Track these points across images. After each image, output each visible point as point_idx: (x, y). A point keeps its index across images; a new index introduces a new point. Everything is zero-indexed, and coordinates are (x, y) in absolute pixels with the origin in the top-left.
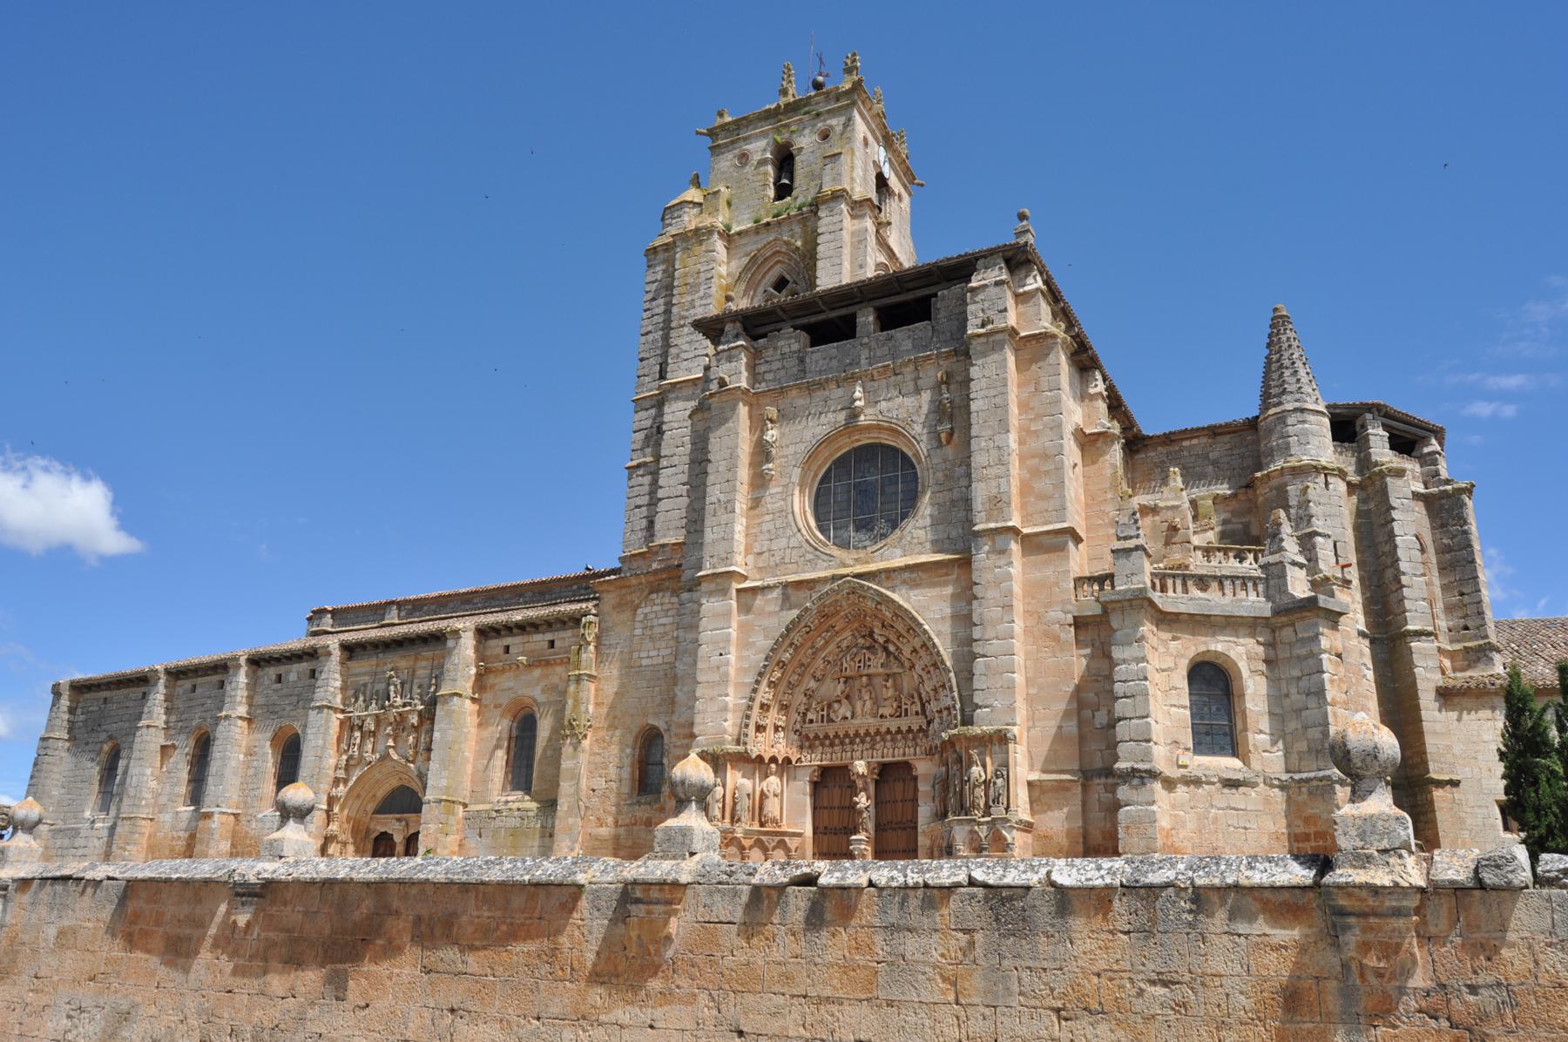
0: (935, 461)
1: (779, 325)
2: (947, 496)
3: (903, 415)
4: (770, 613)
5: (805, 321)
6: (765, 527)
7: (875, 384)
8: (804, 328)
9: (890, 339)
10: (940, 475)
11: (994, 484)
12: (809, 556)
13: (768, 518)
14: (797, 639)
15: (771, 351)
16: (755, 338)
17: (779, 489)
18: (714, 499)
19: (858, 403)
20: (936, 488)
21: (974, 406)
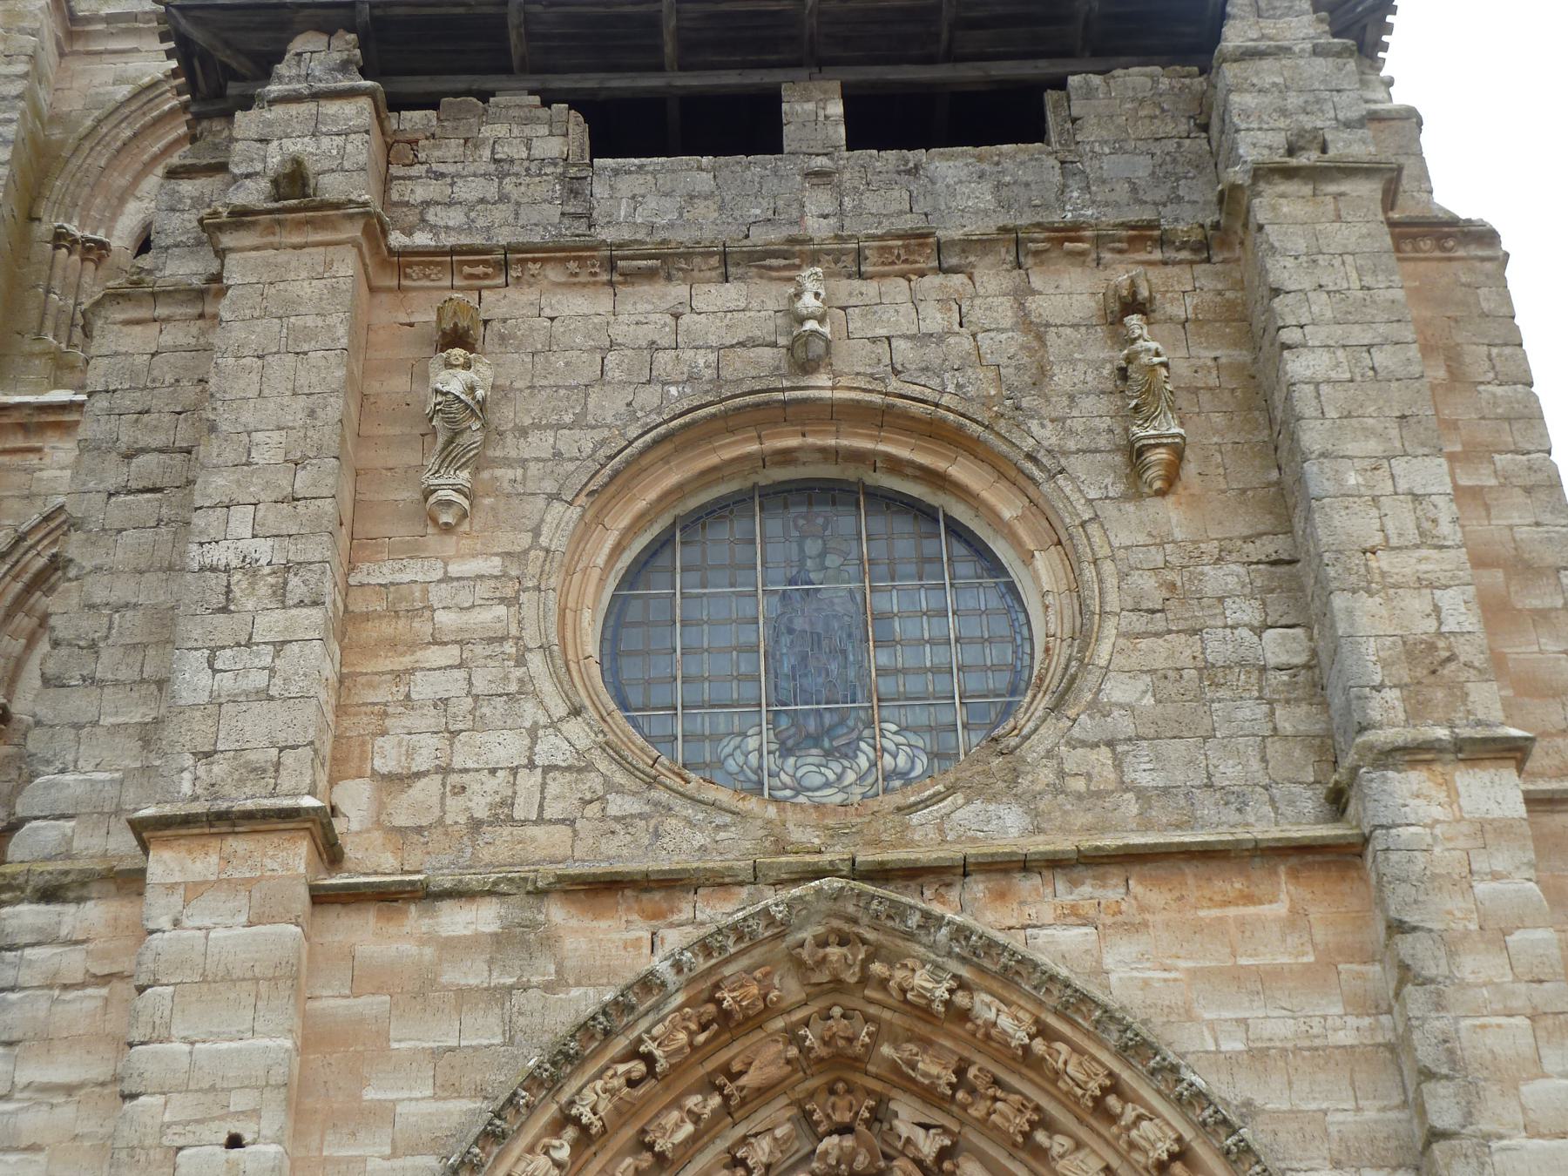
0: (1121, 537)
1: (488, 83)
2: (1184, 649)
3: (981, 383)
4: (463, 995)
5: (590, 82)
6: (423, 688)
7: (871, 288)
8: (577, 102)
9: (914, 171)
10: (1147, 583)
11: (1416, 604)
12: (618, 805)
13: (437, 656)
14: (592, 1097)
15: (453, 147)
16: (397, 104)
17: (493, 565)
18: (220, 554)
19: (811, 325)
20: (1138, 623)
21: (1298, 366)
